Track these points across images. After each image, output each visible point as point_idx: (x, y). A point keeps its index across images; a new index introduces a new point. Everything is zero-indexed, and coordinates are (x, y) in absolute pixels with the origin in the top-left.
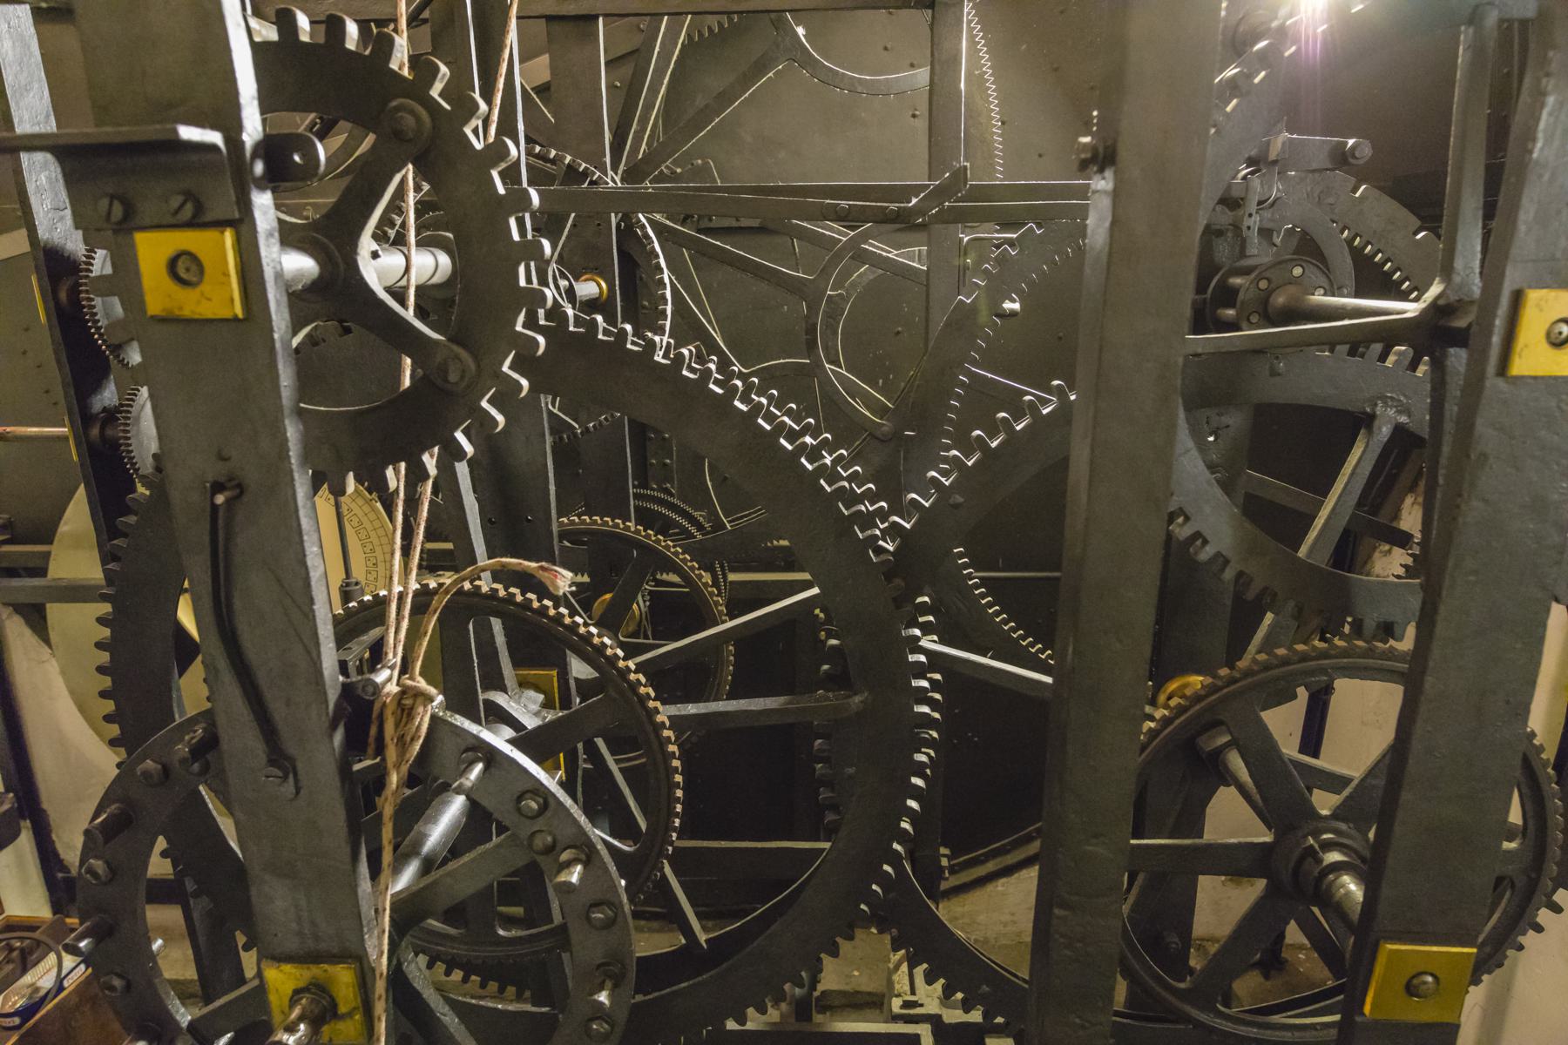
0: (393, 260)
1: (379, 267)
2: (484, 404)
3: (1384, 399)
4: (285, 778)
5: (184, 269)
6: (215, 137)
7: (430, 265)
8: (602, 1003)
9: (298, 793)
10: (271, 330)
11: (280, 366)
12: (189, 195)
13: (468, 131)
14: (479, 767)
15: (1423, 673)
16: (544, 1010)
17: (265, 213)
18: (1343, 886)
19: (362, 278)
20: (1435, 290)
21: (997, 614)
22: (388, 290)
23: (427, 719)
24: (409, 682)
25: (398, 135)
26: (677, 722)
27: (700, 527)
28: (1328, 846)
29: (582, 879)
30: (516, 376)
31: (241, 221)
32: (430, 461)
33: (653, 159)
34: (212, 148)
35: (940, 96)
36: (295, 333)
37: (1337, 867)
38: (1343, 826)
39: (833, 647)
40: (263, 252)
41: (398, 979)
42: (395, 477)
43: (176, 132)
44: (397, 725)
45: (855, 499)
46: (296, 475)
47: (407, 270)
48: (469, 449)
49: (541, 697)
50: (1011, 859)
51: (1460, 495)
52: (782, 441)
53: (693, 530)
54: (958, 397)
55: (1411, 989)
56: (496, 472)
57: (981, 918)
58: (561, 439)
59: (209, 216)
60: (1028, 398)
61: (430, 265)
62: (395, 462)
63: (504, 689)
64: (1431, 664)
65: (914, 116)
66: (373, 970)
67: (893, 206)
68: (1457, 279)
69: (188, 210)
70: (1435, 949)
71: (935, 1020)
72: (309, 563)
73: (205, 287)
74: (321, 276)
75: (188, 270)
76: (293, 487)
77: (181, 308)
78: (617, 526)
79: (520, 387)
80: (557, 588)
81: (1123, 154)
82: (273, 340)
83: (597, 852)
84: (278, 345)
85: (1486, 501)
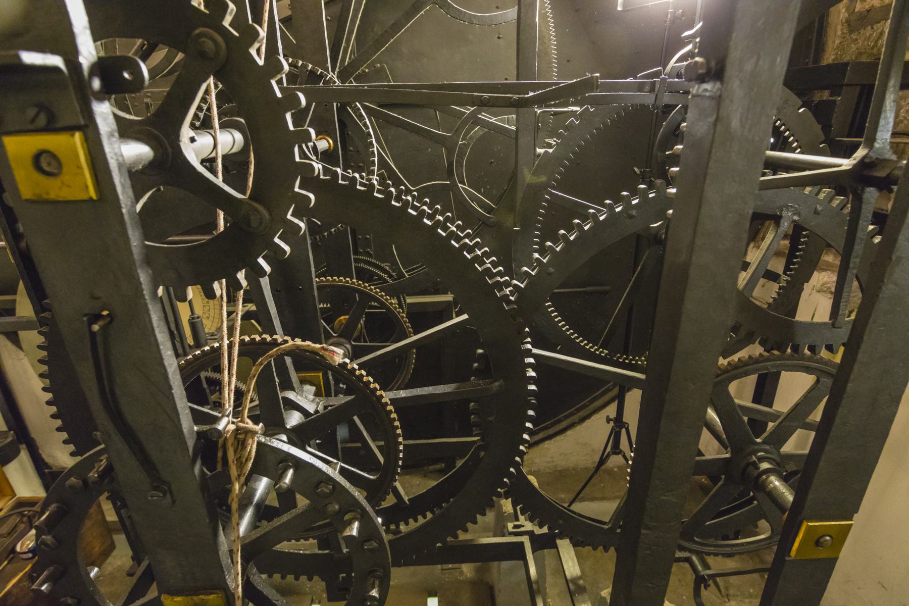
0: (205, 140)
1: (195, 147)
2: (276, 240)
3: (787, 207)
4: (165, 495)
5: (43, 163)
6: (56, 61)
7: (229, 141)
8: (374, 597)
9: (174, 502)
10: (120, 207)
11: (130, 232)
12: (41, 107)
13: (253, 51)
14: (291, 472)
15: (846, 382)
16: (326, 552)
17: (105, 119)
18: (772, 482)
19: (185, 158)
20: (861, 153)
21: (563, 326)
22: (203, 162)
23: (255, 446)
24: (241, 425)
25: (202, 55)
26: (393, 401)
27: (390, 276)
28: (761, 459)
29: (360, 531)
30: (296, 221)
31: (86, 126)
32: (241, 276)
33: (354, 65)
34: (56, 69)
35: (523, 26)
36: (137, 201)
37: (767, 471)
38: (767, 447)
39: (480, 354)
40: (107, 149)
41: (248, 586)
42: (220, 288)
43: (18, 58)
44: (235, 451)
45: (493, 275)
46: (150, 307)
47: (215, 146)
48: (267, 268)
49: (314, 388)
50: (551, 431)
51: (883, 281)
52: (453, 242)
53: (386, 276)
54: (544, 208)
55: (818, 543)
56: (288, 277)
57: (537, 461)
58: (315, 238)
59: (60, 125)
60: (591, 211)
61: (229, 141)
62: (219, 279)
63: (293, 389)
64: (852, 377)
65: (499, 38)
66: (233, 595)
67: (516, 96)
68: (877, 145)
69: (42, 120)
70: (833, 523)
71: (530, 534)
72: (166, 363)
73: (66, 177)
74: (155, 157)
75: (49, 164)
76: (149, 315)
77: (47, 193)
78: (347, 282)
79: (300, 228)
80: (335, 361)
81: (731, 71)
82: (122, 214)
83: (367, 512)
84: (126, 217)
85: (896, 285)
